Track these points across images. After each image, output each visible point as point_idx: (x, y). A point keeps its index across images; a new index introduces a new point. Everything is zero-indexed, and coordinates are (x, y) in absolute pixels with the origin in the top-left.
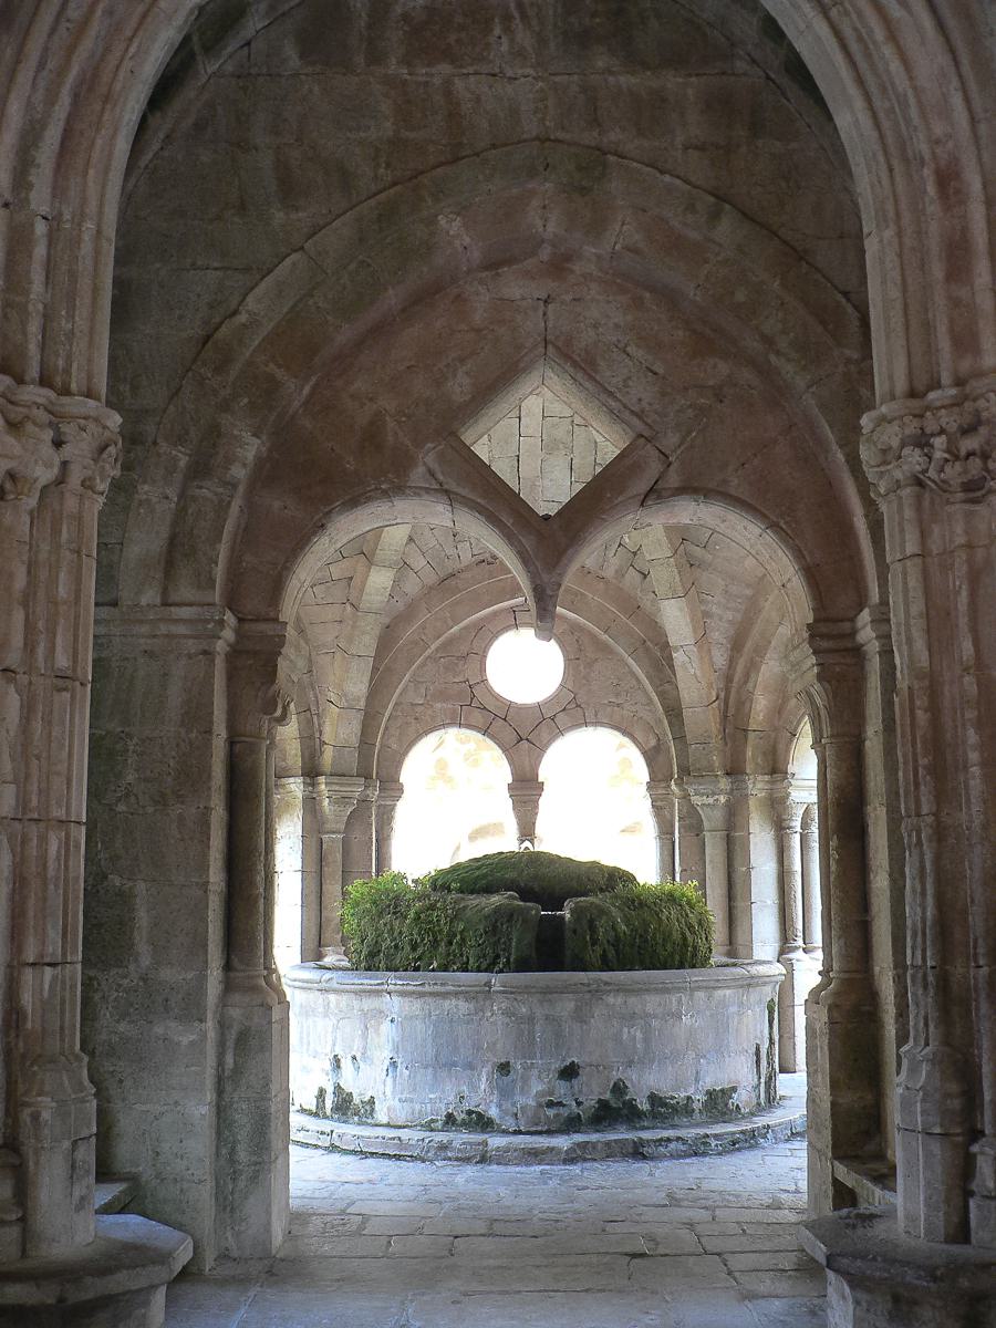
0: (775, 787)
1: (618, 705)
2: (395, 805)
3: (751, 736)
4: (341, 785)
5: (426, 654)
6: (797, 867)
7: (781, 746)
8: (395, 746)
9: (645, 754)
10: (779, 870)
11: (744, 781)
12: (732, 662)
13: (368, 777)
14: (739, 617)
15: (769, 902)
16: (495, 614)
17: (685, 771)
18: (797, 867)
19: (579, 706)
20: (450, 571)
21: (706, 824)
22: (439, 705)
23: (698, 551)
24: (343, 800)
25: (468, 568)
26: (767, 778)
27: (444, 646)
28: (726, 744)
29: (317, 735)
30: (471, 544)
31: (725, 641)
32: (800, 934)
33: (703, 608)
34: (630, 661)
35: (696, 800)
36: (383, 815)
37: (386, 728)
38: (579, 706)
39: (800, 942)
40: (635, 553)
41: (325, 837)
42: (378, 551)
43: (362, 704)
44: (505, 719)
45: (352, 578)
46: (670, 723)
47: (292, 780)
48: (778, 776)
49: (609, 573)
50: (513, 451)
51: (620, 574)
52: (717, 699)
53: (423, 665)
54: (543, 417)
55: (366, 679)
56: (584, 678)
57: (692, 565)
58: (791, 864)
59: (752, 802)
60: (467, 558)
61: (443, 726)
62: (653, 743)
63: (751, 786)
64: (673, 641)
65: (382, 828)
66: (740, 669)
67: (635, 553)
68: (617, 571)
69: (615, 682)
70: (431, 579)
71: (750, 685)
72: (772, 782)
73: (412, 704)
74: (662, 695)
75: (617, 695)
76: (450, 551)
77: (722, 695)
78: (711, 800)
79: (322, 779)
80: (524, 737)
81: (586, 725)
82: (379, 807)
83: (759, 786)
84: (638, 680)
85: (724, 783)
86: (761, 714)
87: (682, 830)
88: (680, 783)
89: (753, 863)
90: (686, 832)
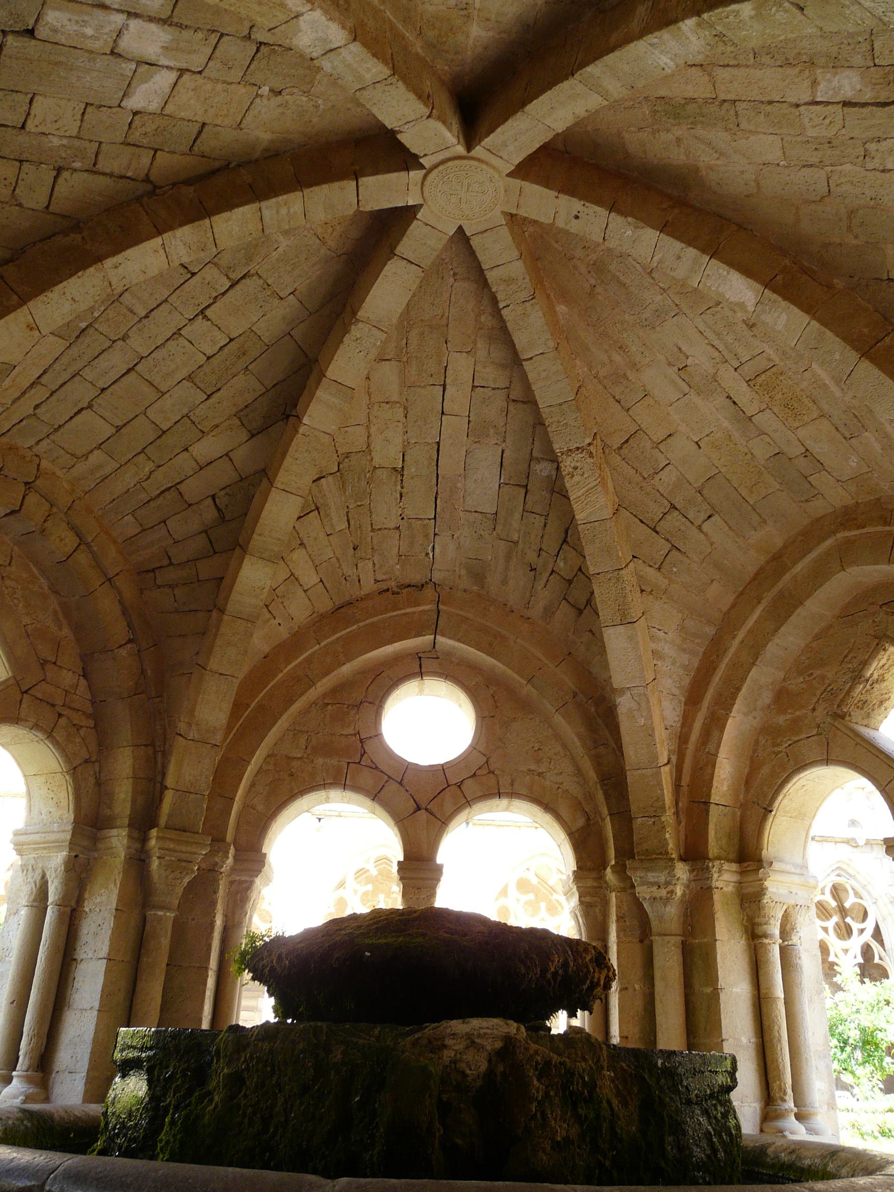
0: (745, 879)
1: (539, 774)
2: (251, 883)
3: (713, 808)
4: (179, 842)
5: (313, 694)
6: (779, 992)
7: (751, 827)
8: (260, 808)
9: (571, 835)
10: (754, 996)
11: (708, 868)
12: (687, 720)
13: (218, 840)
14: (696, 663)
15: (744, 1040)
16: (396, 659)
17: (626, 852)
18: (779, 992)
19: (493, 772)
20: (348, 599)
21: (655, 924)
22: (320, 761)
23: (651, 573)
24: (180, 865)
25: (367, 597)
26: (734, 867)
27: (336, 691)
28: (679, 823)
29: (159, 778)
30: (374, 564)
31: (677, 692)
32: (789, 1091)
33: (653, 646)
34: (558, 719)
35: (643, 892)
36: (237, 893)
37: (253, 785)
38: (491, 772)
39: (790, 1104)
40: (570, 582)
41: (150, 913)
42: (255, 536)
43: (218, 738)
44: (400, 783)
45: (222, 579)
46: (607, 796)
47: (114, 832)
48: (752, 865)
49: (537, 611)
50: (433, 440)
51: (549, 612)
52: (668, 763)
53: (306, 712)
54: (474, 387)
55: (227, 706)
56: (500, 740)
57: (642, 591)
58: (770, 987)
59: (717, 896)
60: (369, 585)
61: (324, 786)
62: (581, 822)
63: (715, 876)
64: (618, 680)
65: (233, 913)
66: (697, 726)
67: (570, 582)
68: (545, 609)
69: (537, 747)
70: (325, 605)
71: (711, 747)
72: (742, 873)
73: (288, 758)
74: (597, 760)
75: (538, 761)
76: (349, 571)
77: (674, 759)
78: (663, 893)
79: (154, 832)
80: (424, 806)
81: (499, 795)
82: (232, 883)
83: (726, 876)
84: (565, 746)
85: (682, 871)
86: (726, 783)
87: (622, 934)
88: (621, 870)
89: (721, 983)
90: (625, 936)
